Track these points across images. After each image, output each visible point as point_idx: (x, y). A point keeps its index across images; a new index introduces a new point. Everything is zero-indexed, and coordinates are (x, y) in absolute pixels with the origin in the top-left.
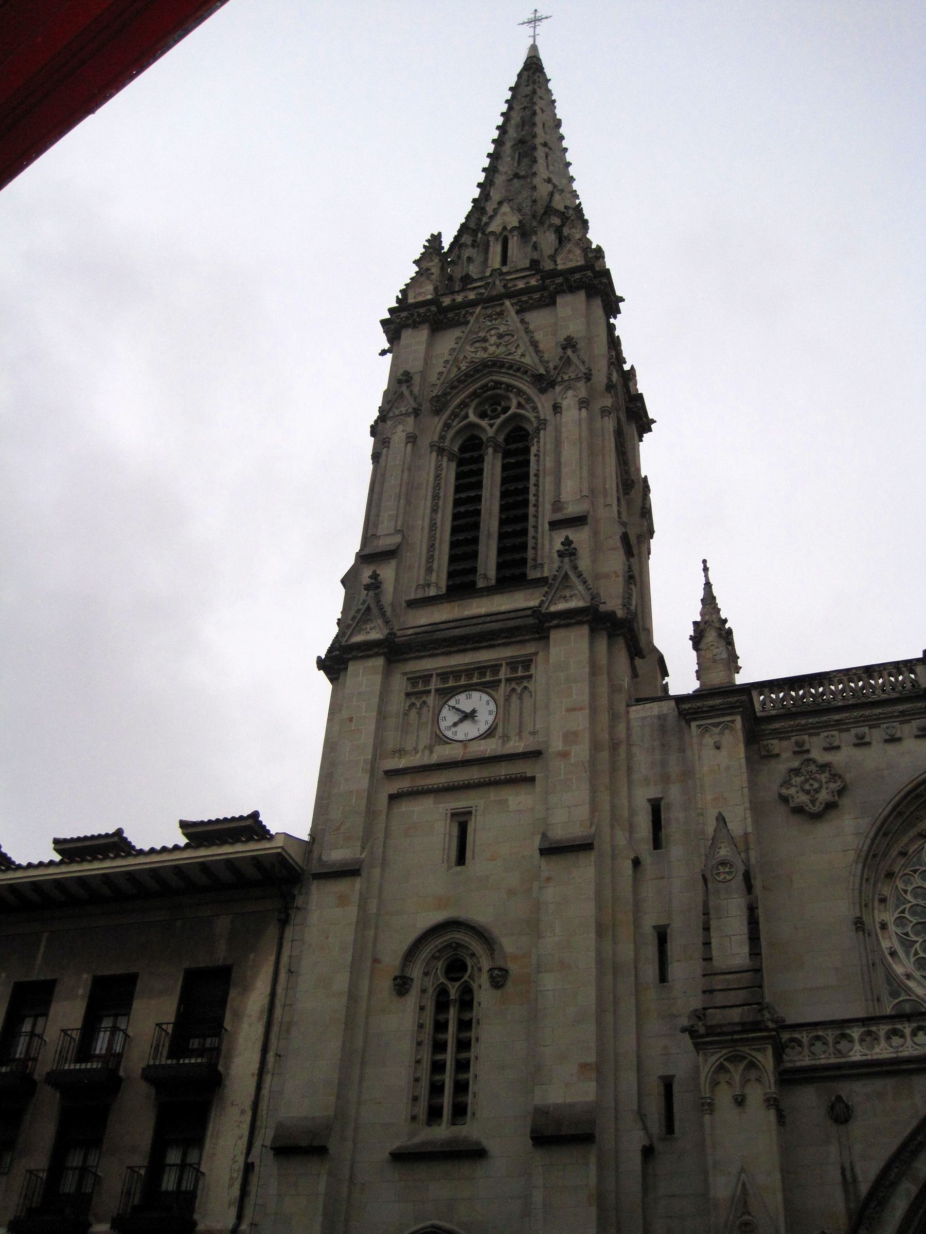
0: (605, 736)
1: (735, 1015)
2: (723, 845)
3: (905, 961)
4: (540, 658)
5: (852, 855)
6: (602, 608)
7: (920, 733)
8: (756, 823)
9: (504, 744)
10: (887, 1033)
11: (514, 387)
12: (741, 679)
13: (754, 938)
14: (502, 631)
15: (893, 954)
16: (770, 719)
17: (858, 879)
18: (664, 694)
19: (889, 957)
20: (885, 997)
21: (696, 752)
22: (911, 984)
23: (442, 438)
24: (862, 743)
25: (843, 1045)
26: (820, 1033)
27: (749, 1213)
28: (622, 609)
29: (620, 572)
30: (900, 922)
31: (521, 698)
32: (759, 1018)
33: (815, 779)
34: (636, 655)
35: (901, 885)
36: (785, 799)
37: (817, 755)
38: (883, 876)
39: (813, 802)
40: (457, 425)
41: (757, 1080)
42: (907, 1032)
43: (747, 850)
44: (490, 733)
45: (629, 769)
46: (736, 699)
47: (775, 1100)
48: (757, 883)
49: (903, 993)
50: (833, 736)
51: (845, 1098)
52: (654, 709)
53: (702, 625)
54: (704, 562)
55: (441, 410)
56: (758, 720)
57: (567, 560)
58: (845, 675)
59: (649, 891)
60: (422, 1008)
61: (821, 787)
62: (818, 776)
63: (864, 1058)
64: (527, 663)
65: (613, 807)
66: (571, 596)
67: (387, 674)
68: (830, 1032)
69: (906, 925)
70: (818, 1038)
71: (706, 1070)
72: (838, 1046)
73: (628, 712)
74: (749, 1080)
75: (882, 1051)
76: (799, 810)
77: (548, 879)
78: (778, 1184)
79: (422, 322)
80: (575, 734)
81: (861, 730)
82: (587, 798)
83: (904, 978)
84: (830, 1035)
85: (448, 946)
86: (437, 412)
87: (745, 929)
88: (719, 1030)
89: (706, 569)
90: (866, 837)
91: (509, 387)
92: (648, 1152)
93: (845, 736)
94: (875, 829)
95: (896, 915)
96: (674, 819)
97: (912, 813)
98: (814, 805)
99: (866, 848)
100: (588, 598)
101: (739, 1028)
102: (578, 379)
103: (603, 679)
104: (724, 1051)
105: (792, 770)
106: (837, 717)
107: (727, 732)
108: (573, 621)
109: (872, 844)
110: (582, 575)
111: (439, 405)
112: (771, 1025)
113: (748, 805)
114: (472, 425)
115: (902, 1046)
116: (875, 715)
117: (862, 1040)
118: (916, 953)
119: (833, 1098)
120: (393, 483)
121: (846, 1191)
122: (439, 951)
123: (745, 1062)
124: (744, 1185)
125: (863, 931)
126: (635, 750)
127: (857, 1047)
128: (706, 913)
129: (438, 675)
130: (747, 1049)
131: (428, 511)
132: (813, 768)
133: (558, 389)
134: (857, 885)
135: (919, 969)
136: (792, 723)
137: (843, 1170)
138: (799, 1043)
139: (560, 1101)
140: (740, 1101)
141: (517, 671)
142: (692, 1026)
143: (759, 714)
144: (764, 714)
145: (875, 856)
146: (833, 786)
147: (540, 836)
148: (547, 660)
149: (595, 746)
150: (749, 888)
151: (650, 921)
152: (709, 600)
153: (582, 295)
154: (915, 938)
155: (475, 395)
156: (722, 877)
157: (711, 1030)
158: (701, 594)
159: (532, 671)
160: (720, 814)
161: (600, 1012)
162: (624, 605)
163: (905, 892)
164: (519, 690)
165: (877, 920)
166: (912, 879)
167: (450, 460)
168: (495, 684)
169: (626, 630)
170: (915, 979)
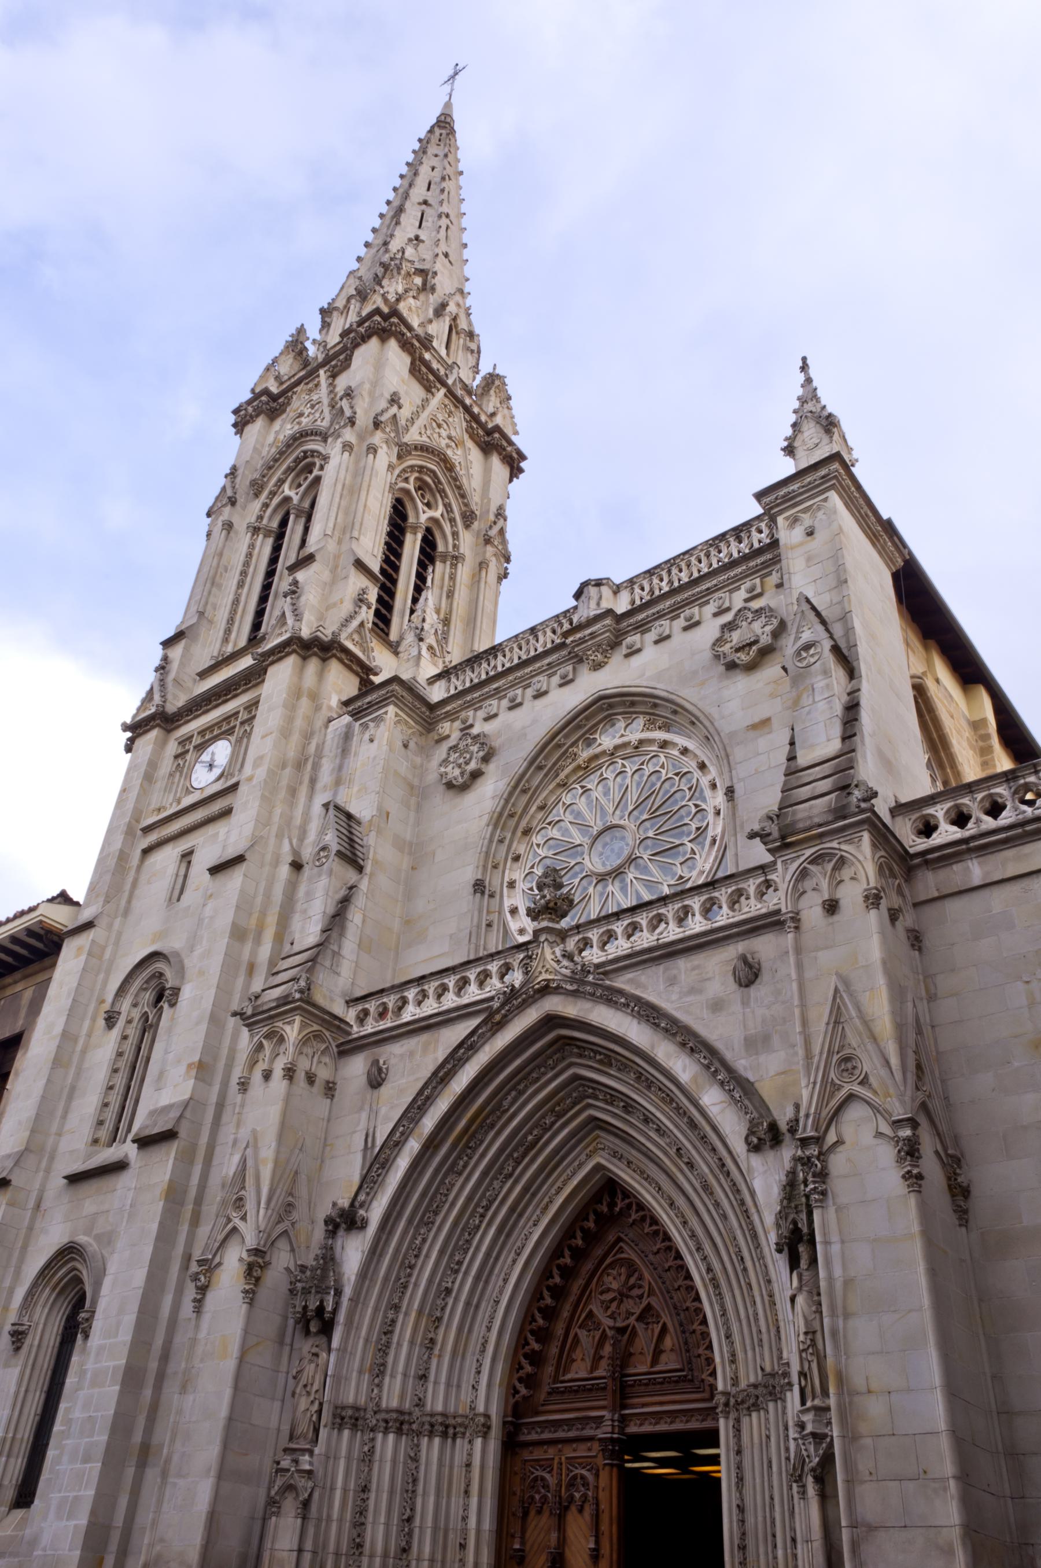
0: (292, 754)
5: (486, 819)
7: (562, 681)
11: (318, 452)
17: (486, 841)
19: (508, 915)
23: (260, 518)
24: (515, 706)
33: (467, 752)
39: (462, 774)
40: (276, 500)
45: (313, 781)
51: (381, 1062)
55: (260, 492)
56: (432, 707)
57: (288, 598)
60: (125, 1038)
61: (471, 759)
64: (255, 703)
65: (288, 821)
67: (162, 744)
74: (278, 1054)
76: (450, 785)
79: (257, 416)
83: (515, 934)
85: (153, 976)
86: (257, 495)
91: (313, 451)
94: (509, 788)
97: (555, 764)
98: (462, 777)
99: (498, 809)
102: (345, 426)
104: (265, 1029)
106: (495, 686)
111: (257, 487)
114: (287, 499)
120: (206, 569)
122: (147, 982)
129: (199, 733)
131: (234, 588)
133: (330, 440)
134: (484, 849)
146: (481, 754)
153: (374, 342)
155: (289, 470)
165: (506, 879)
167: (265, 536)
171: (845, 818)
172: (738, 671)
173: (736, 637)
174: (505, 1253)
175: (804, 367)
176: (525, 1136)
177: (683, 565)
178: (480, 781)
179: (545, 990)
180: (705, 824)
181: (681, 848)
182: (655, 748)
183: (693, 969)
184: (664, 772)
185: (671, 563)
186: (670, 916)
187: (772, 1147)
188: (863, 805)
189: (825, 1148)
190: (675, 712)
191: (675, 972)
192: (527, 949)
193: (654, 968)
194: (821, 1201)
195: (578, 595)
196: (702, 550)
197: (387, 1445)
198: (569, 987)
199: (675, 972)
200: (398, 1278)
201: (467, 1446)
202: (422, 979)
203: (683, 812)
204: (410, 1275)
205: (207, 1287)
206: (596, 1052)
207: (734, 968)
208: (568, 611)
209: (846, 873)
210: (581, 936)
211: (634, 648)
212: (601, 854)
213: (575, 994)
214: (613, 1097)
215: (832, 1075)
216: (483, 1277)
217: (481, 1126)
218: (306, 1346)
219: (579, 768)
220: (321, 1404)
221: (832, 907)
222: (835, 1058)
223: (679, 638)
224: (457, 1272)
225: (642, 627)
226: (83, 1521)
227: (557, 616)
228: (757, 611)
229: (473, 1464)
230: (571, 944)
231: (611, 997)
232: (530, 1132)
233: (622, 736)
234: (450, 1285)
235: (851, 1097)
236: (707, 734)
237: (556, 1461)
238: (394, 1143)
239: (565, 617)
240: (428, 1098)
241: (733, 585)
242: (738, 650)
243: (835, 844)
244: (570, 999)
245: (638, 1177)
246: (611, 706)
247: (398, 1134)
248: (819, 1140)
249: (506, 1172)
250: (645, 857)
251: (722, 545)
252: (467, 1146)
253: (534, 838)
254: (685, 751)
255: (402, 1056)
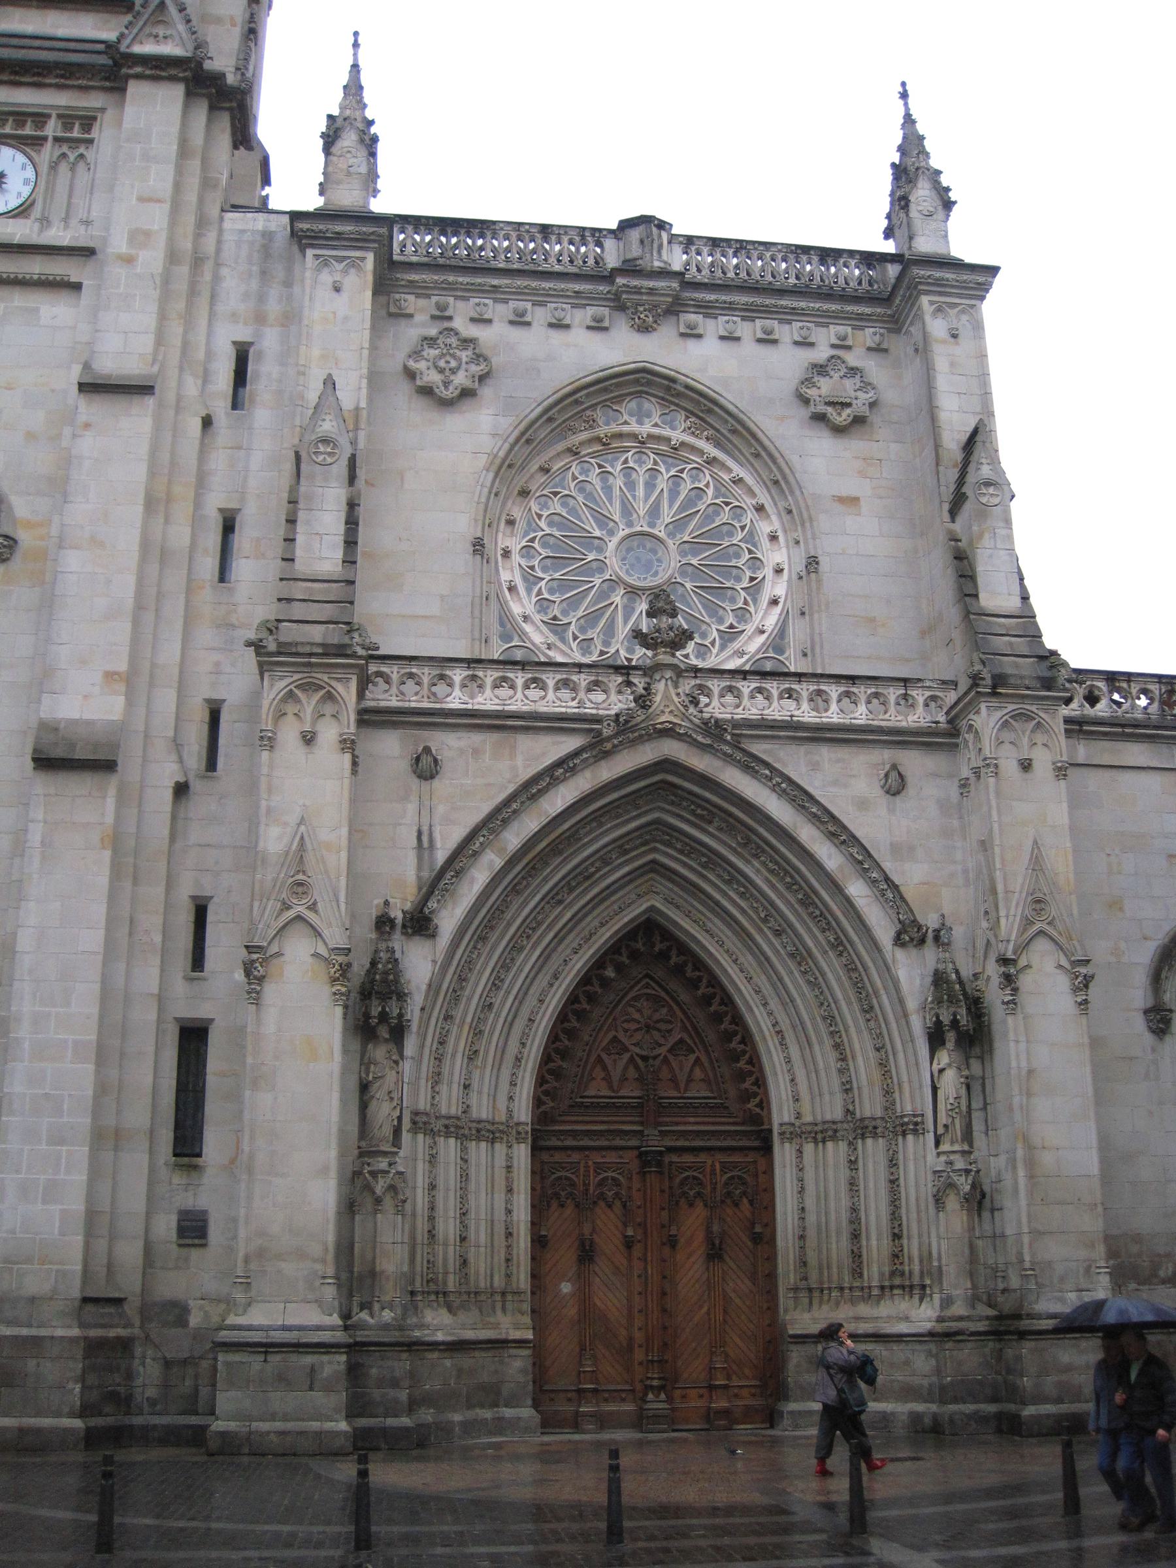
0: (186, 245)
1: (317, 634)
2: (328, 417)
3: (525, 601)
4: (109, 115)
5: (483, 460)
6: (208, 65)
8: (370, 399)
9: (41, 231)
10: (495, 680)
12: (378, 206)
13: (350, 543)
14: (57, 65)
15: (512, 589)
16: (410, 266)
17: (486, 490)
18: (263, 207)
19: (506, 591)
20: (495, 640)
21: (308, 290)
22: (528, 628)
24: (520, 321)
25: (441, 689)
26: (414, 670)
27: (304, 873)
28: (235, 74)
29: (239, 20)
30: (527, 550)
31: (73, 169)
32: (346, 640)
33: (453, 356)
34: (241, 144)
35: (535, 508)
36: (411, 375)
37: (459, 323)
38: (516, 492)
39: (446, 384)
41: (333, 716)
42: (520, 682)
43: (357, 429)
44: (22, 211)
45: (213, 297)
46: (372, 230)
47: (353, 742)
48: (361, 473)
49: (516, 638)
50: (485, 305)
52: (259, 222)
53: (339, 122)
54: (356, 34)
56: (393, 264)
58: (514, 230)
59: (218, 461)
61: (458, 368)
62: (458, 353)
63: (464, 706)
64: (88, 121)
65: (186, 346)
66: (165, 38)
68: (426, 671)
69: (533, 557)
70: (411, 676)
71: (272, 697)
72: (434, 689)
73: (222, 219)
75: (487, 700)
76: (427, 391)
77: (87, 426)
78: (344, 843)
80: (148, 234)
81: (521, 305)
82: (153, 324)
83: (520, 620)
84: (426, 674)
87: (341, 528)
88: (294, 650)
89: (356, 45)
90: (505, 441)
92: (181, 790)
93: (500, 308)
94: (516, 433)
95: (524, 543)
96: (264, 372)
97: (564, 422)
98: (446, 388)
99: (502, 454)
100: (191, 47)
101: (320, 651)
103: (195, 164)
104: (296, 676)
105: (426, 338)
106: (495, 282)
107: (353, 271)
108: (163, 74)
109: (511, 450)
110: (185, 9)
112: (361, 652)
113: (365, 371)
115: (511, 698)
116: (544, 289)
117: (464, 686)
118: (539, 593)
119: (420, 749)
121: (420, 858)
123: (322, 692)
124: (302, 838)
125: (482, 557)
126: (224, 271)
127: (457, 692)
128: (293, 502)
130: (325, 677)
132: (453, 341)
134: (483, 500)
135: (539, 612)
136: (436, 278)
137: (420, 834)
138: (388, 681)
139: (76, 715)
140: (309, 739)
141: (71, 130)
142: (261, 640)
143: (395, 257)
144: (402, 258)
145: (510, 466)
146: (475, 369)
147: (80, 367)
148: (119, 123)
149: (173, 257)
150: (352, 478)
151: (216, 501)
152: (354, 89)
154: (540, 575)
156: (321, 458)
157: (284, 649)
158: (344, 79)
159: (94, 134)
160: (330, 375)
161: (139, 607)
162: (238, 69)
163: (540, 516)
164: (72, 157)
165: (501, 545)
166: (550, 503)
168: (37, 142)
169: (234, 104)
170: (533, 623)
171: (1049, 689)
172: (822, 425)
173: (825, 387)
174: (540, 976)
175: (904, 95)
176: (586, 869)
177: (755, 254)
178: (467, 403)
179: (668, 732)
180: (761, 577)
181: (730, 592)
182: (698, 460)
183: (838, 761)
184: (710, 492)
185: (742, 247)
186: (805, 694)
187: (915, 946)
188: (1067, 685)
189: (1018, 968)
190: (734, 431)
191: (817, 758)
192: (628, 674)
193: (794, 747)
194: (1013, 1009)
195: (626, 225)
196: (780, 251)
197: (449, 1148)
198: (700, 738)
199: (817, 758)
200: (454, 991)
201: (504, 1150)
202: (471, 662)
203: (731, 550)
204: (462, 988)
205: (264, 977)
206: (699, 806)
207: (887, 775)
208: (600, 230)
209: (1040, 738)
210: (698, 682)
211: (694, 332)
212: (624, 559)
213: (702, 747)
214: (692, 848)
215: (1027, 911)
216: (521, 998)
217: (552, 850)
218: (379, 1052)
219: (598, 439)
220: (401, 1109)
221: (1026, 766)
222: (1030, 898)
223: (749, 347)
224: (498, 988)
225: (708, 310)
226: (78, 1206)
227: (584, 229)
228: (852, 369)
229: (515, 1164)
230: (687, 685)
231: (752, 765)
232: (592, 864)
233: (656, 425)
234: (493, 1000)
235: (1041, 932)
236: (779, 477)
237: (582, 1165)
238: (464, 851)
239: (593, 236)
240: (515, 812)
241: (824, 319)
242: (829, 403)
243: (1033, 708)
244: (695, 750)
245: (697, 928)
246: (649, 383)
247: (478, 844)
248: (1014, 962)
249: (560, 897)
250: (688, 585)
251: (804, 258)
252: (533, 868)
253: (532, 503)
254: (738, 481)
255: (462, 751)
